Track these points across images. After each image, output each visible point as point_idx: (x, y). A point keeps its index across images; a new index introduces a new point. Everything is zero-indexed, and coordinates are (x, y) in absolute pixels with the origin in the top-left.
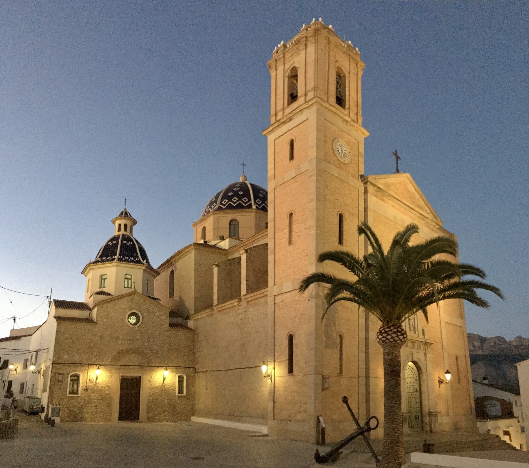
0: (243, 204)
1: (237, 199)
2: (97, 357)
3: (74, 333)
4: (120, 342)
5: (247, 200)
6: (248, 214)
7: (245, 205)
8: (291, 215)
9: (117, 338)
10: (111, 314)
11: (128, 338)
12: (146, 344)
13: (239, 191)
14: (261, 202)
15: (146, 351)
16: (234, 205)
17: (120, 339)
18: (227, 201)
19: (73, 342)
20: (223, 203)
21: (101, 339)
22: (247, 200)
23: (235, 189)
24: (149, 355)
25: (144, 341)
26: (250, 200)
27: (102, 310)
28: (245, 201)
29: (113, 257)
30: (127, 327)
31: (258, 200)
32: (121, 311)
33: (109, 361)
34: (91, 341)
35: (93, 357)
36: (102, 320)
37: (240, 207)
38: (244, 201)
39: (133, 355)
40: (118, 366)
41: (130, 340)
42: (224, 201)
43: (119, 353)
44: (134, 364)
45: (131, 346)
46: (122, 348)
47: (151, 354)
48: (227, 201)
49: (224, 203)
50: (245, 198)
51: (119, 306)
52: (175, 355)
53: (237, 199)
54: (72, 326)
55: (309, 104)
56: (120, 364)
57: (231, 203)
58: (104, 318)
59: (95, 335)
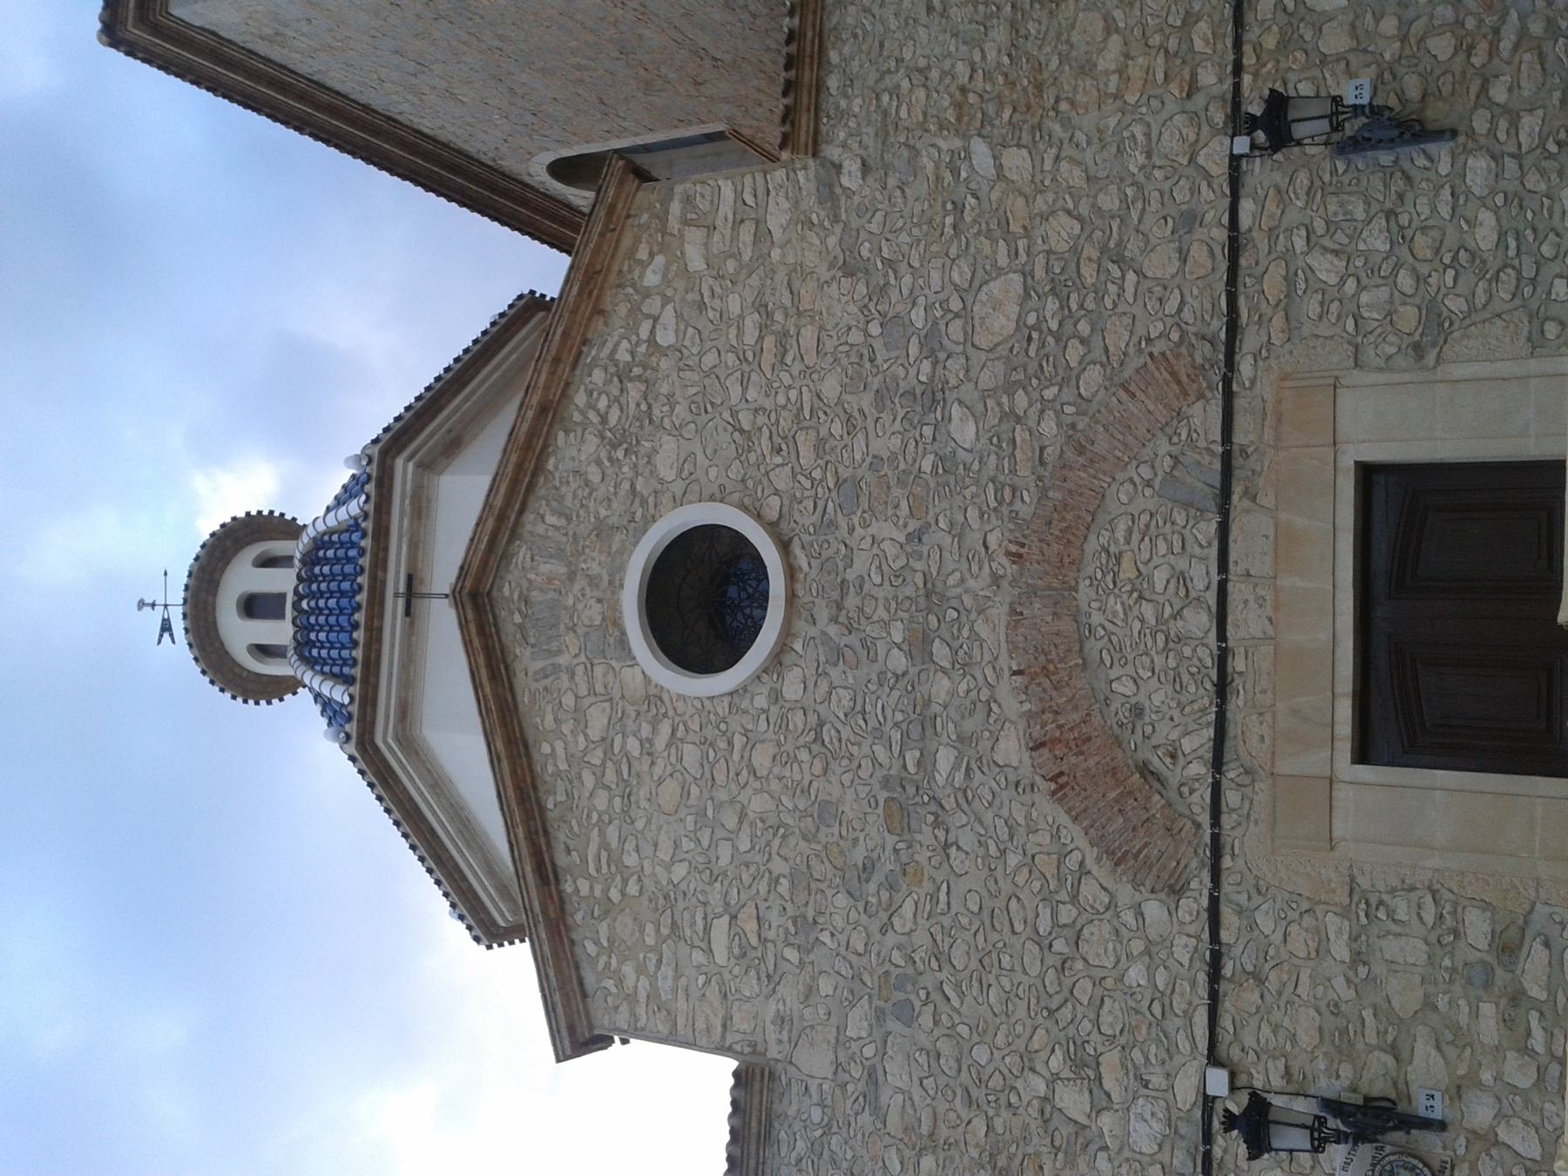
4: (945, 759)
10: (668, 868)
11: (898, 661)
15: (1049, 426)
17: (911, 757)
21: (907, 1015)
25: (927, 465)
27: (628, 970)
30: (792, 689)
32: (633, 745)
33: (1154, 910)
39: (1085, 592)
40: (1231, 797)
41: (918, 647)
43: (1060, 785)
44: (1202, 575)
45: (992, 630)
46: (1011, 749)
47: (1074, 352)
51: (589, 780)
56: (1198, 769)
58: (699, 957)
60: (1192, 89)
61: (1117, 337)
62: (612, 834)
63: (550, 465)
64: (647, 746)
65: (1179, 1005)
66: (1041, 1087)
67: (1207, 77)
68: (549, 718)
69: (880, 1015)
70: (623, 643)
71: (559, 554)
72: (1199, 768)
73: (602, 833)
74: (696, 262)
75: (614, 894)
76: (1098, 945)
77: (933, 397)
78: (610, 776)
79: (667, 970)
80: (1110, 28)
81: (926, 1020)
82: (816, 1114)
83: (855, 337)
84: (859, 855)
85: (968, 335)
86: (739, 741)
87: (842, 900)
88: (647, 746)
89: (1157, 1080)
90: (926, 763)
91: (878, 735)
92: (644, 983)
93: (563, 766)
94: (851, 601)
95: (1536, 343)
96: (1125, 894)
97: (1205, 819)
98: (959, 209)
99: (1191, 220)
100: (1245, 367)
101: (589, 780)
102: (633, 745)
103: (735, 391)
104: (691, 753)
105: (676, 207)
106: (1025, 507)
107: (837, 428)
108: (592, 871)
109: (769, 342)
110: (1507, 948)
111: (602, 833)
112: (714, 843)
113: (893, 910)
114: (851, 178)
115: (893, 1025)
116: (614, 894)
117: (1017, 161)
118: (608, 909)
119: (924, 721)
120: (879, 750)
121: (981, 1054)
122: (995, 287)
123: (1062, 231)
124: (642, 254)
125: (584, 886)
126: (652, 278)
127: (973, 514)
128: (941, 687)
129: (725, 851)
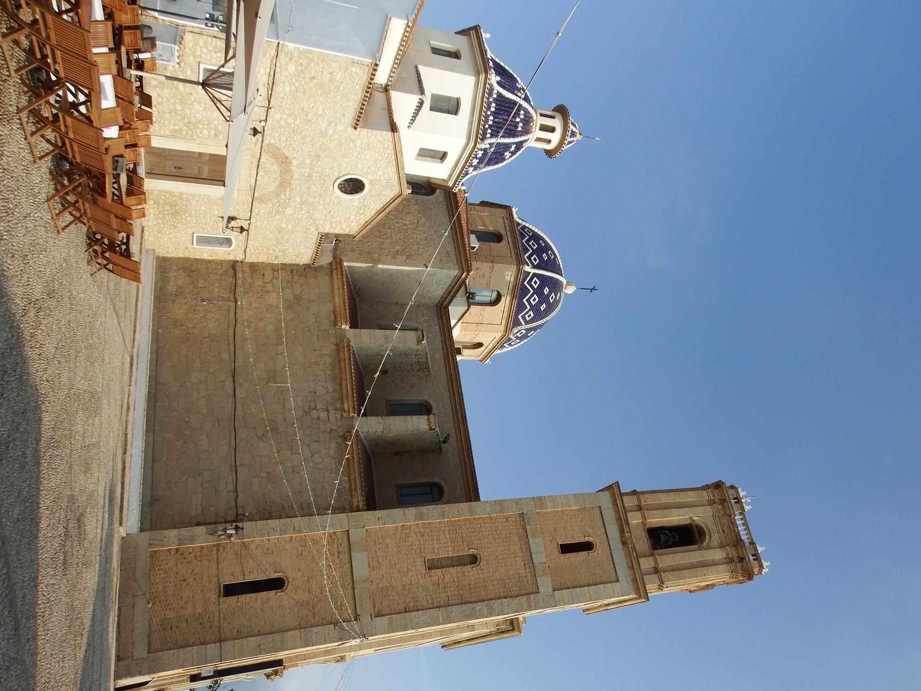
0: (523, 313)
1: (533, 303)
2: (283, 123)
3: (342, 88)
4: (308, 162)
5: (528, 319)
6: (504, 322)
7: (520, 317)
8: (474, 560)
9: (318, 157)
12: (298, 199)
13: (548, 303)
14: (520, 336)
15: (283, 197)
16: (524, 300)
17: (314, 162)
18: (536, 287)
19: (321, 86)
20: (535, 279)
22: (528, 319)
23: (553, 294)
24: (275, 201)
26: (527, 323)
28: (526, 316)
29: (489, 131)
30: (336, 174)
31: (524, 332)
32: (373, 169)
33: (272, 141)
34: (319, 116)
35: (284, 117)
36: (361, 137)
37: (521, 308)
38: (529, 314)
42: (537, 280)
43: (287, 158)
44: (259, 178)
45: (296, 176)
46: (295, 162)
47: (277, 205)
48: (536, 287)
49: (532, 283)
50: (532, 315)
52: (271, 236)
53: (533, 303)
54: (357, 87)
55: (639, 584)
57: (530, 294)
58: (364, 141)
59: (329, 125)
60: (256, 227)
61: (270, 205)
62: (380, 158)
63: (382, 205)
64: (369, 168)
65: (270, 131)
66: (296, 122)
67: (254, 228)
68: (391, 174)
69: (326, 133)
70: (371, 182)
71: (382, 194)
72: (262, 157)
73: (383, 157)
74: (344, 226)
75: (382, 150)
76: (283, 138)
77: (302, 203)
78: (378, 166)
79: (371, 141)
80: (268, 236)
81: (317, 132)
82: (342, 120)
83: (315, 212)
84: (327, 153)
85: (295, 209)
86: (349, 168)
87: (331, 147)
88: (369, 168)
89: (275, 122)
90: (311, 162)
91: (320, 166)
92: (378, 138)
93: (389, 168)
94: (322, 182)
95: (209, 196)
96: (278, 145)
97: (263, 152)
98: (295, 222)
99: (258, 214)
100: (251, 199)
101: (384, 166)
102: (373, 169)
103: (340, 209)
104: (360, 166)
105: (347, 231)
106: (288, 190)
107: (321, 202)
108: (386, 154)
109: (332, 213)
110: (216, 135)
111: (383, 157)
112: (357, 156)
113: (321, 145)
114: (313, 229)
115: (324, 131)
116: (382, 150)
117: (284, 225)
118: (384, 148)
119: (311, 167)
120: (320, 164)
121: (307, 127)
122: (290, 213)
123: (277, 217)
124: (355, 227)
125: (389, 152)
126: (354, 224)
127: (298, 189)
128: (307, 170)
129: (355, 154)
